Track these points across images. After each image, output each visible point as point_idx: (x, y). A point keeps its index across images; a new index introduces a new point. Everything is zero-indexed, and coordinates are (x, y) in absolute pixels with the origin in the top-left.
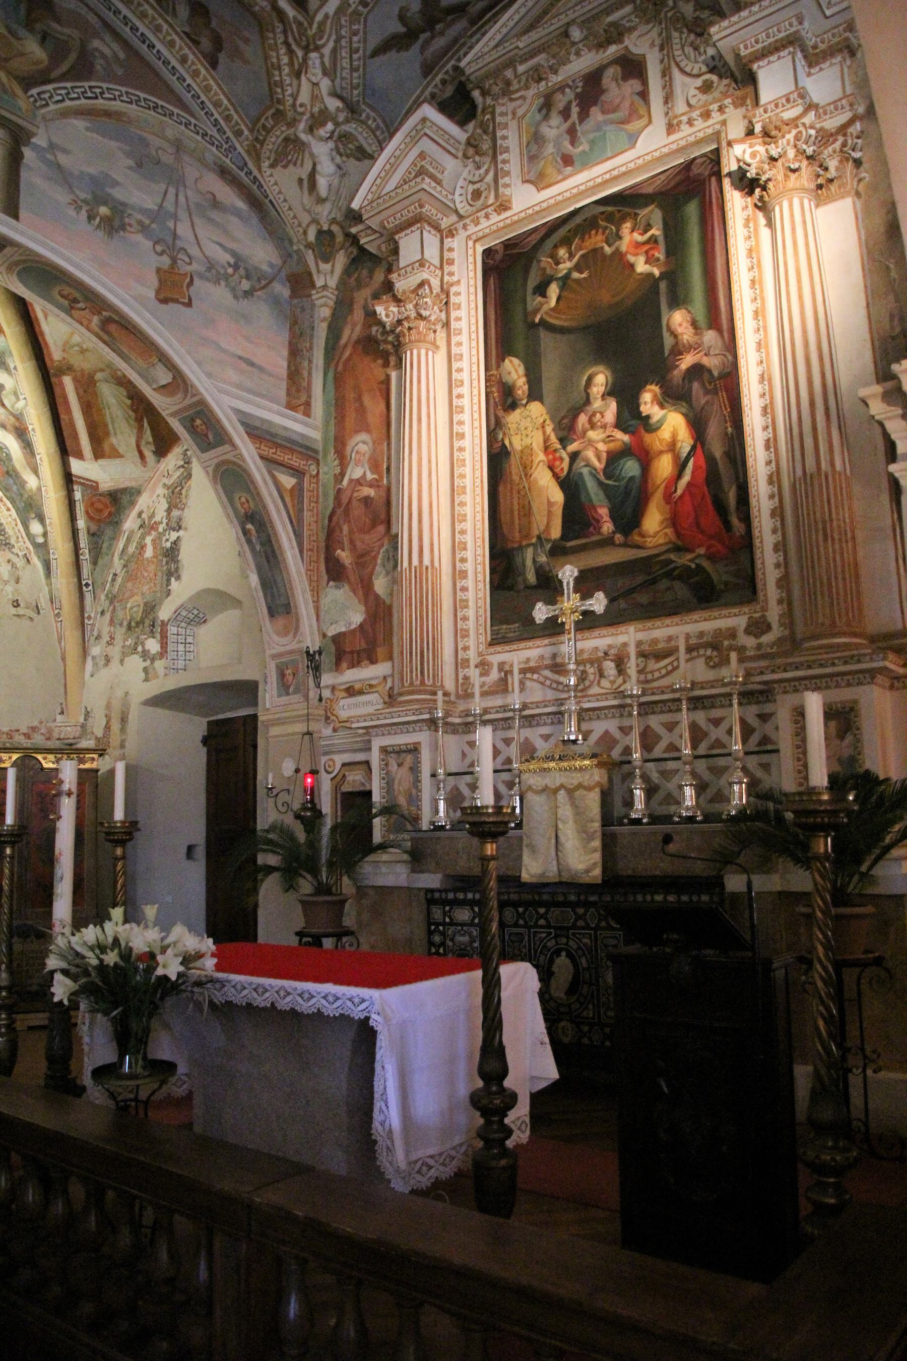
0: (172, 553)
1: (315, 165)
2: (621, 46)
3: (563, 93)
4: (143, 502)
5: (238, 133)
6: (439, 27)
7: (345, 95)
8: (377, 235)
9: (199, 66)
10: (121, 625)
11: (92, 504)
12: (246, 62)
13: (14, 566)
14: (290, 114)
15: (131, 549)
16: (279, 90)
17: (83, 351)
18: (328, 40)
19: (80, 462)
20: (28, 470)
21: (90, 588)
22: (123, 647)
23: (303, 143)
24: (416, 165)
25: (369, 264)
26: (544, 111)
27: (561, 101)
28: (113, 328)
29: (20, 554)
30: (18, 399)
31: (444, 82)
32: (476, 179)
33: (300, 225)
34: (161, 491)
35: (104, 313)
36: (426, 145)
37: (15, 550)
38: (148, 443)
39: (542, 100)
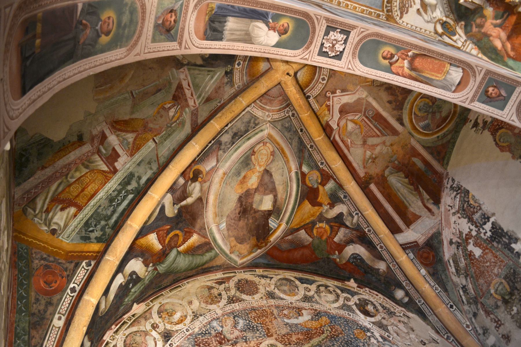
0: (498, 233)
4: (447, 235)
5: (379, 16)
10: (497, 307)
11: (421, 257)
13: (404, 323)
15: (462, 263)
17: (374, 159)
19: (402, 234)
20: (376, 260)
21: (454, 307)
22: (513, 317)
25: (477, 16)
28: (418, 62)
29: (401, 315)
30: (353, 217)
33: (430, 32)
34: (453, 219)
35: (410, 54)
37: (398, 314)
38: (428, 200)
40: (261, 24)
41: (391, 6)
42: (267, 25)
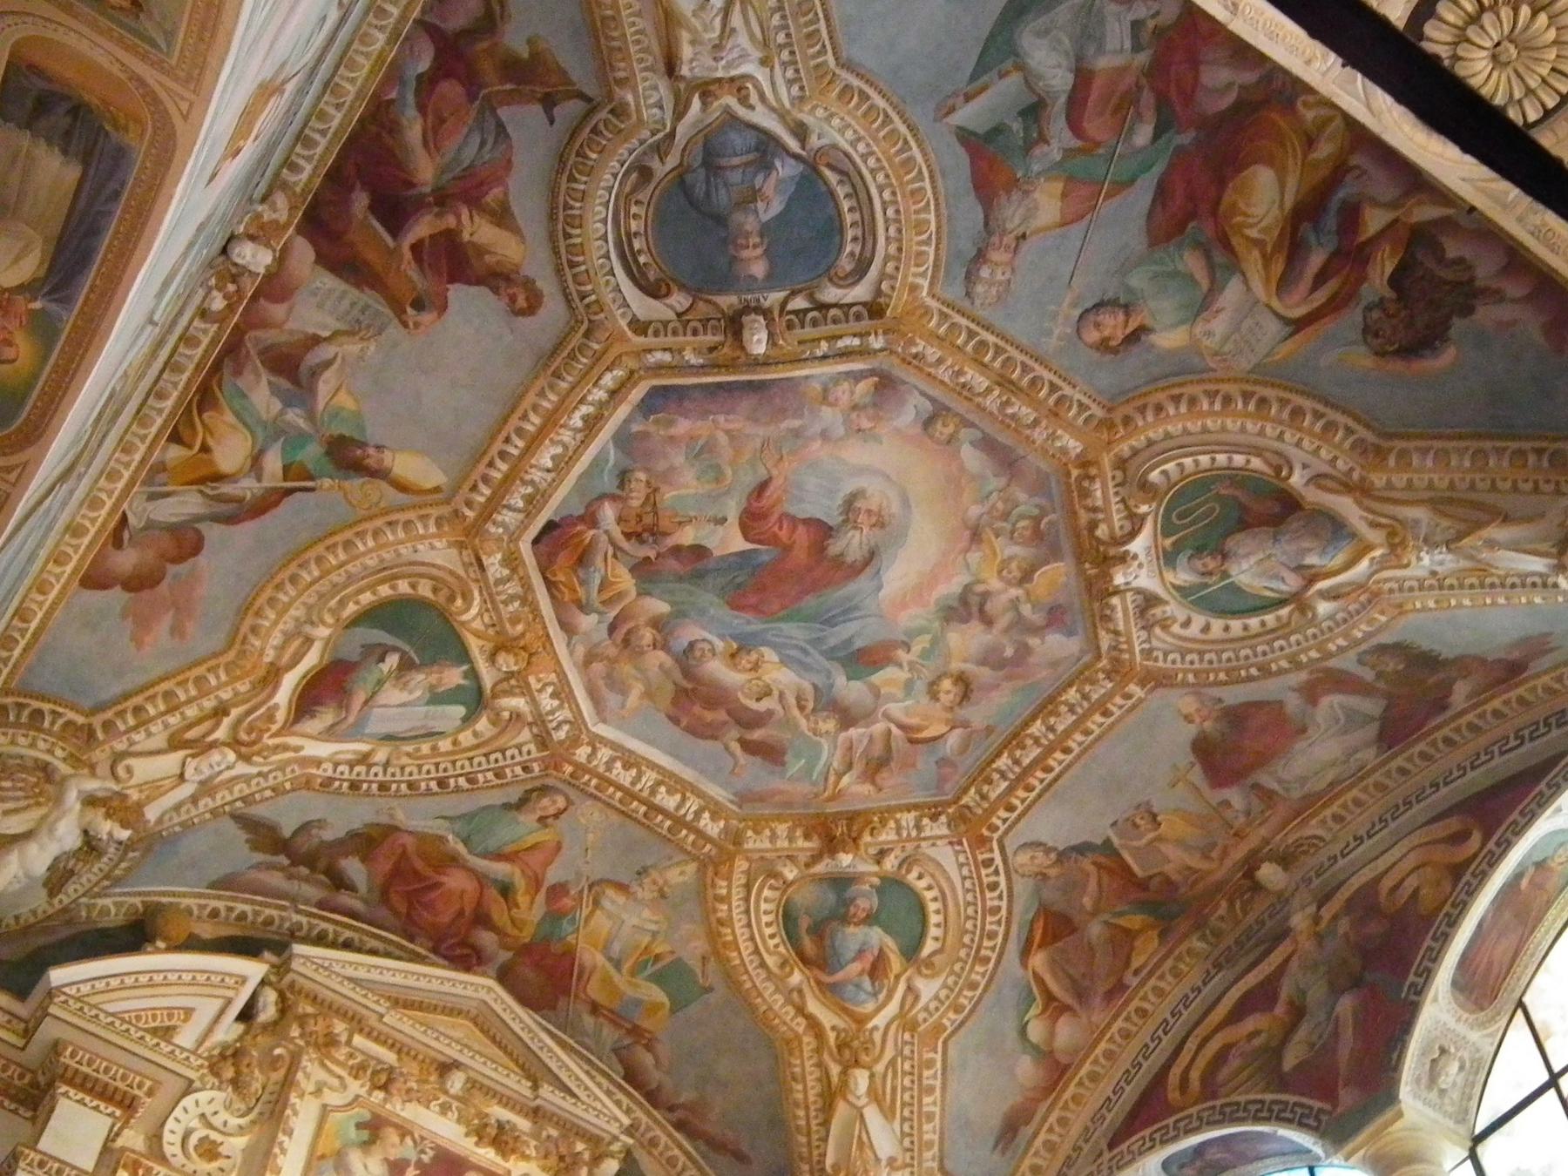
1: (28, 836)
2: (499, 1160)
3: (403, 1136)
6: (304, 870)
7: (167, 817)
8: (20, 1043)
9: (76, 558)
12: (138, 643)
14: (100, 755)
16: (131, 721)
18: (260, 765)
23: (58, 800)
24: (170, 1016)
26: (365, 1135)
27: (395, 1146)
31: (215, 914)
32: (217, 1121)
36: (207, 1009)
39: (367, 1116)
40: (29, 267)
41: (17, 725)
42: (21, 288)
